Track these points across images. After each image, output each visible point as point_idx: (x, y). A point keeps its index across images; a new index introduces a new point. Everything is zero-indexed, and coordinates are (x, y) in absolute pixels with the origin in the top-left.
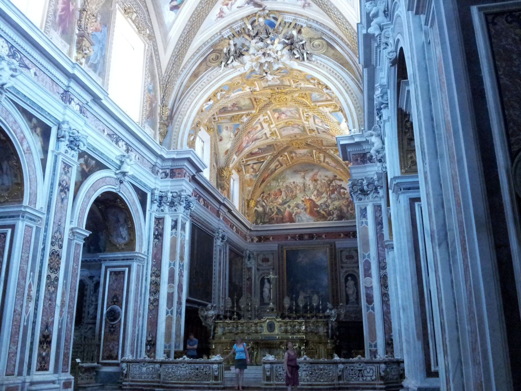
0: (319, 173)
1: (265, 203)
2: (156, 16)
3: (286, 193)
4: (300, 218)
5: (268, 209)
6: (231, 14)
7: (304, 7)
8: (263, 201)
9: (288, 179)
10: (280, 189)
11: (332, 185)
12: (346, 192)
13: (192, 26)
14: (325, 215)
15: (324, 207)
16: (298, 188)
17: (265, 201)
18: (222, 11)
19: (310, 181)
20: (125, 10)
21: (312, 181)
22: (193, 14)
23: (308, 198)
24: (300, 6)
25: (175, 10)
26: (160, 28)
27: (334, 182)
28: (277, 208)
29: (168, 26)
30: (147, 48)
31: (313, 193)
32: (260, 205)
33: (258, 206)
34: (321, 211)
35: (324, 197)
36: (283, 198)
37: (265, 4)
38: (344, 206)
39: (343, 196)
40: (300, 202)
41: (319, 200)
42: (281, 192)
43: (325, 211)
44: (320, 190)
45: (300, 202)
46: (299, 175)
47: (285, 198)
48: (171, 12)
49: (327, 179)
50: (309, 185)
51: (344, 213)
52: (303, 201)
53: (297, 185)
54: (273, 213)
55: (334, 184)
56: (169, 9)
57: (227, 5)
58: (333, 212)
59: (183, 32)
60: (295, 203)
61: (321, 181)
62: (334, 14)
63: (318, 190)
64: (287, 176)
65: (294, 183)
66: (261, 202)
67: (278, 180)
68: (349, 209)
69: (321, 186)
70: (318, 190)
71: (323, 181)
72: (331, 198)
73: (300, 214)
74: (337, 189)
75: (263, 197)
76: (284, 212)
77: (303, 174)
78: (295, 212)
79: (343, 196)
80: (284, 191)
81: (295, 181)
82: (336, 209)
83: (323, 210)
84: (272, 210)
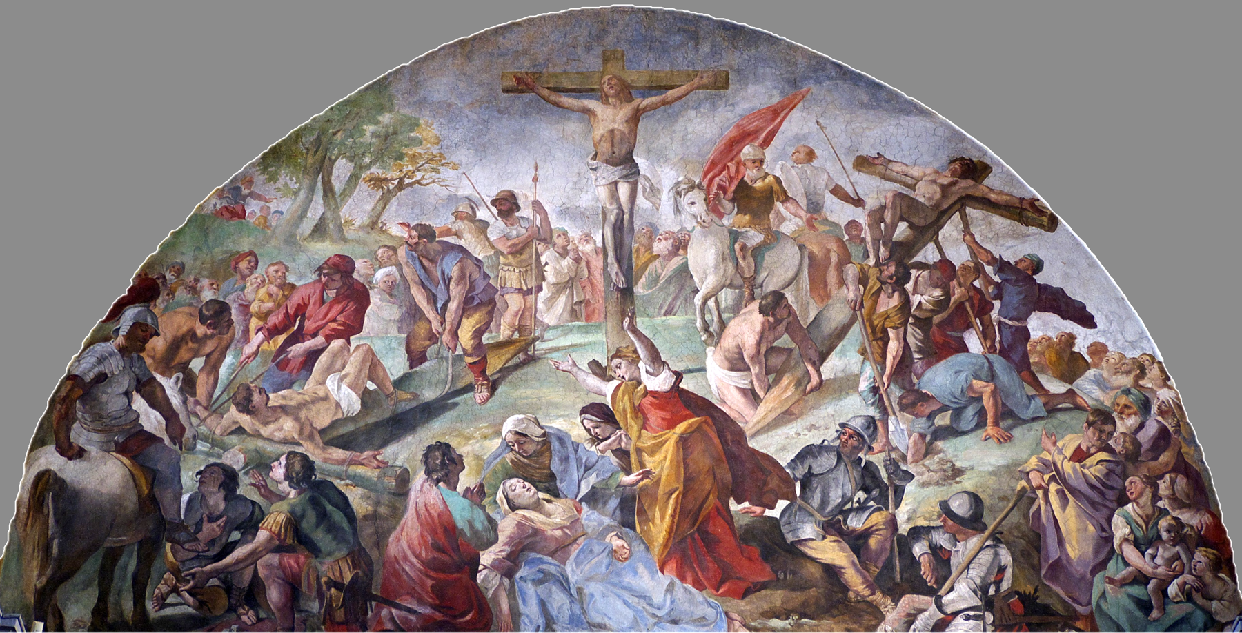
0: (796, 124)
1: (157, 401)
3: (414, 313)
4: (558, 600)
5: (188, 478)
8: (147, 388)
9: (438, 161)
10: (342, 267)
11: (929, 254)
12: (1084, 339)
14: (854, 579)
15: (841, 487)
16: (554, 266)
17: (170, 386)
19: (696, 205)
21: (714, 207)
23: (660, 383)
27: (950, 230)
28: (303, 473)
31: (714, 333)
32: (100, 422)
33: (80, 435)
34: (808, 530)
35: (847, 384)
36: (373, 366)
38: (1068, 490)
39: (1056, 387)
40: (575, 428)
41: (787, 416)
42: (358, 297)
43: (857, 542)
44: (799, 300)
45: (575, 428)
46: (573, 126)
47: (395, 365)
49: (874, 190)
50: (680, 245)
51: (1058, 568)
52: (602, 413)
53: (544, 235)
54: (250, 526)
55: (959, 255)
58: (941, 558)
60: (509, 426)
61: (815, 207)
63: (774, 305)
64: (430, 129)
65: (507, 205)
66: (112, 399)
67: (323, 168)
68: (1120, 529)
69: (817, 267)
70: (774, 305)
71: (840, 213)
72: (915, 400)
73: (561, 549)
74: (983, 309)
75: (141, 334)
76: (385, 521)
77: (610, 117)
78: (507, 526)
79: (1056, 387)
80: (391, 289)
81: (525, 194)
82: (974, 523)
83: (833, 526)
84: (246, 488)
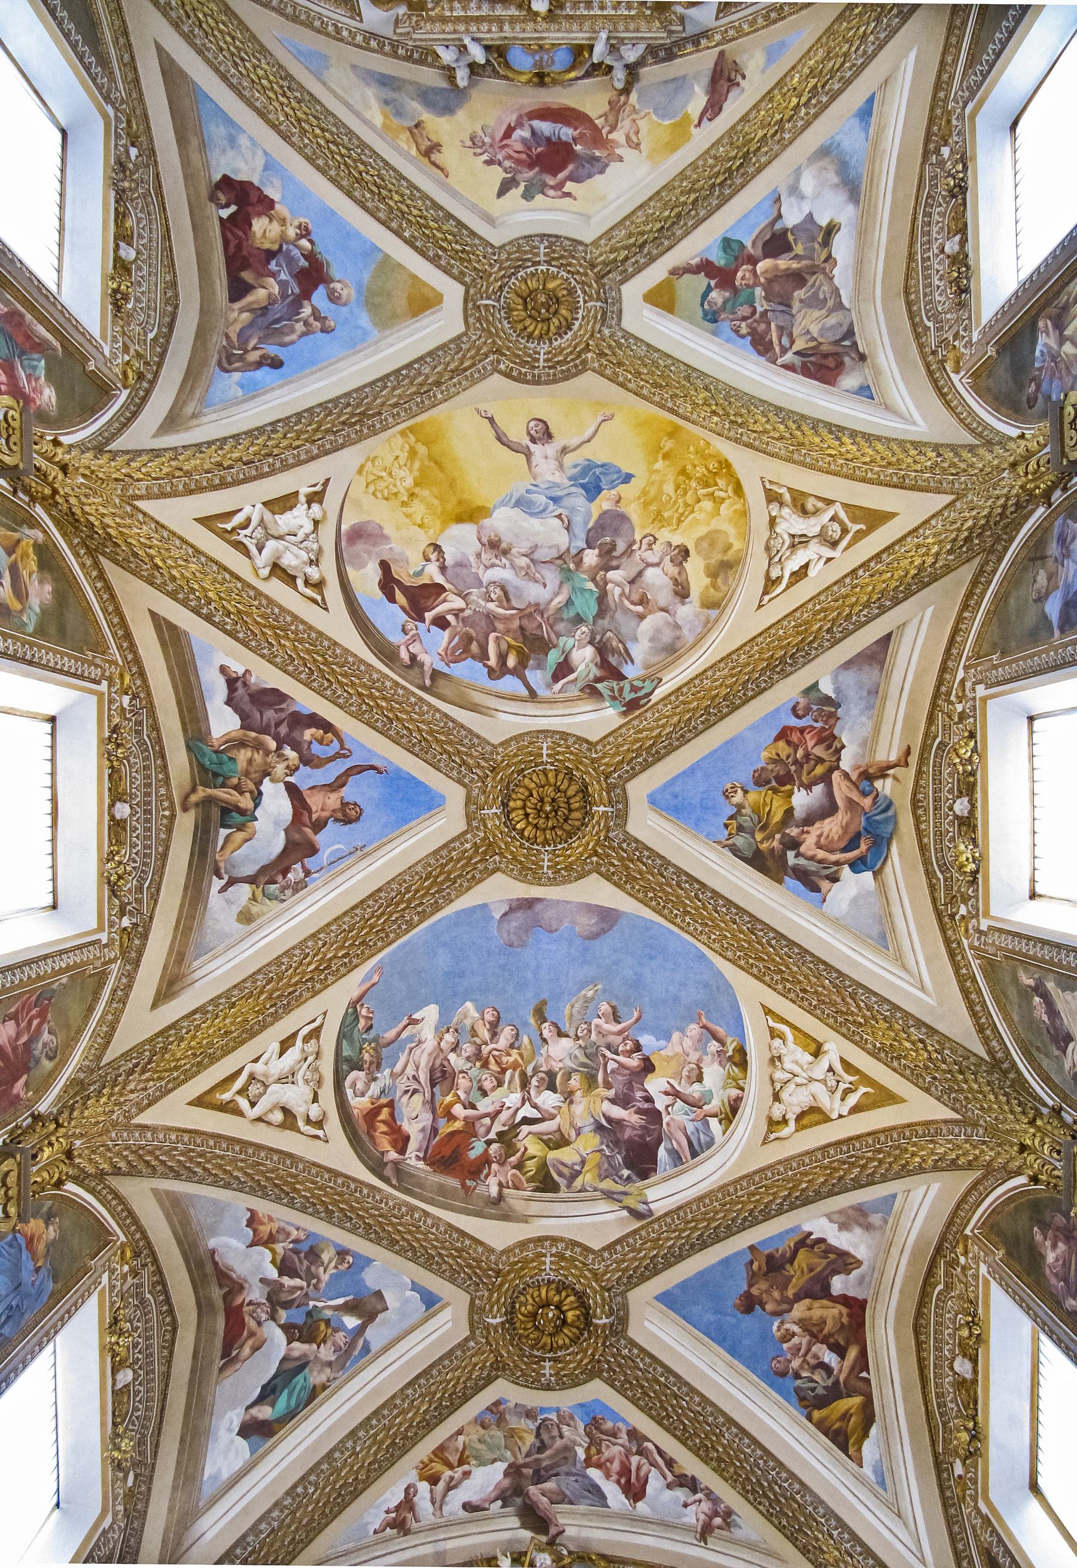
2: (182, 1441)
6: (434, 1528)
7: (705, 1532)
13: (293, 1513)
18: (408, 1503)
20: (115, 1321)
22: (311, 1471)
24: (687, 1529)
25: (254, 1438)
26: (175, 1488)
29: (207, 1490)
30: (107, 1523)
37: (561, 1520)
48: (242, 1443)
56: (237, 1430)
57: (434, 1480)
59: (254, 1529)
62: (831, 1536)
